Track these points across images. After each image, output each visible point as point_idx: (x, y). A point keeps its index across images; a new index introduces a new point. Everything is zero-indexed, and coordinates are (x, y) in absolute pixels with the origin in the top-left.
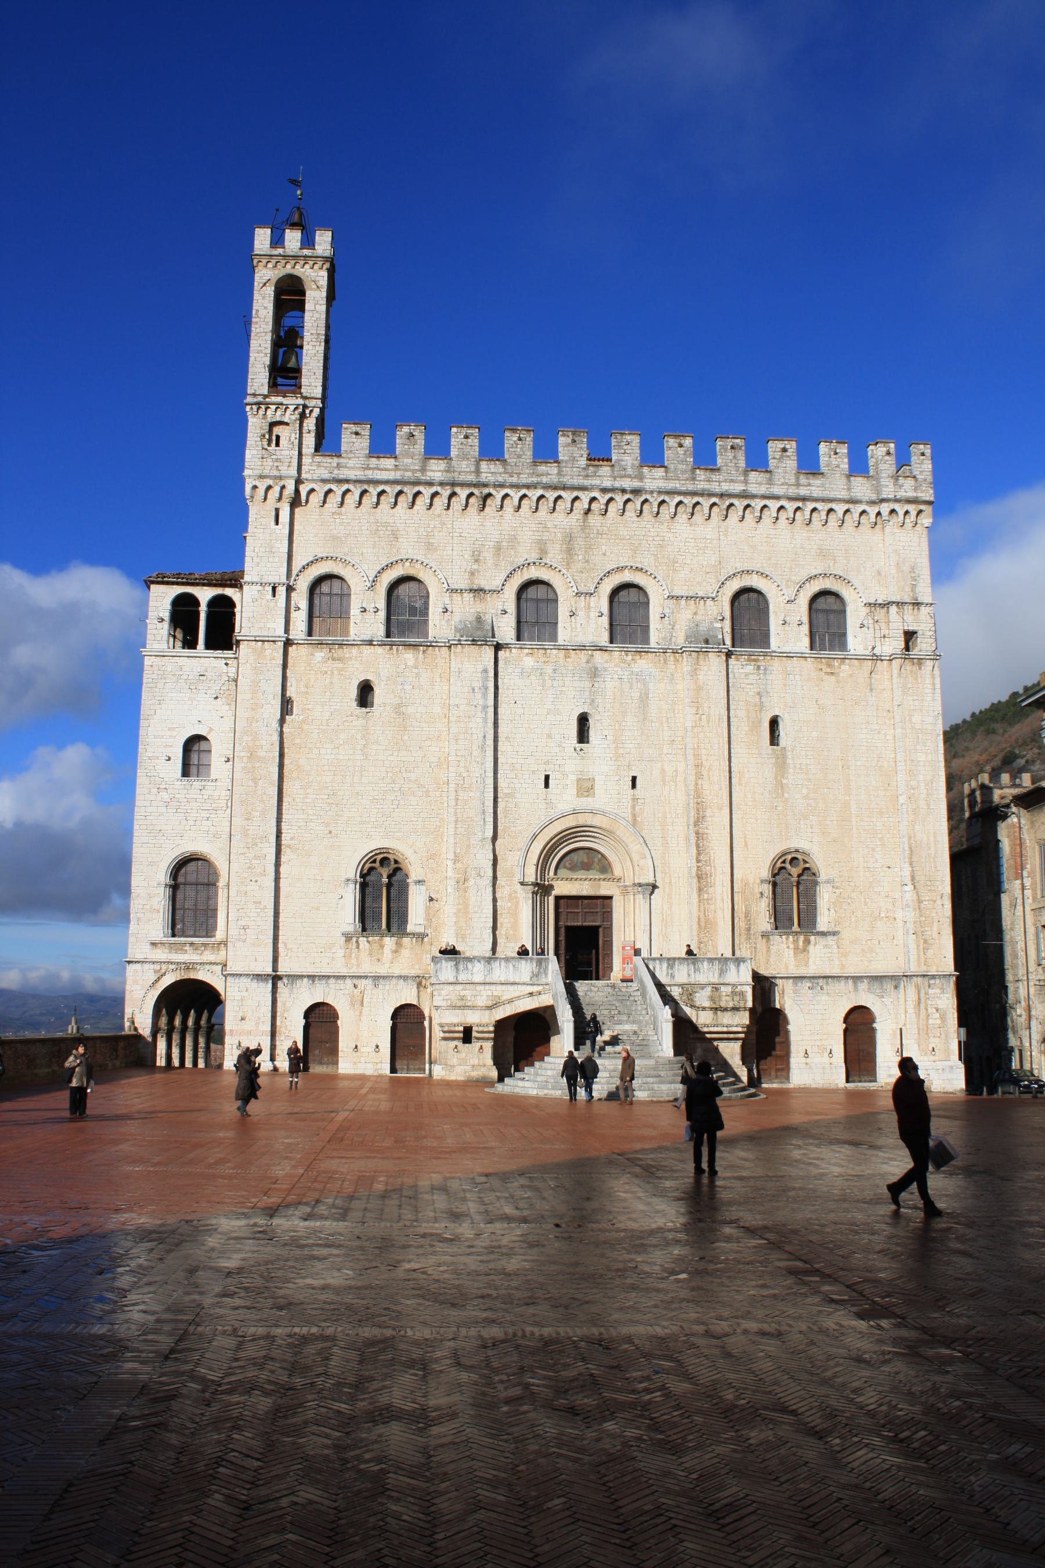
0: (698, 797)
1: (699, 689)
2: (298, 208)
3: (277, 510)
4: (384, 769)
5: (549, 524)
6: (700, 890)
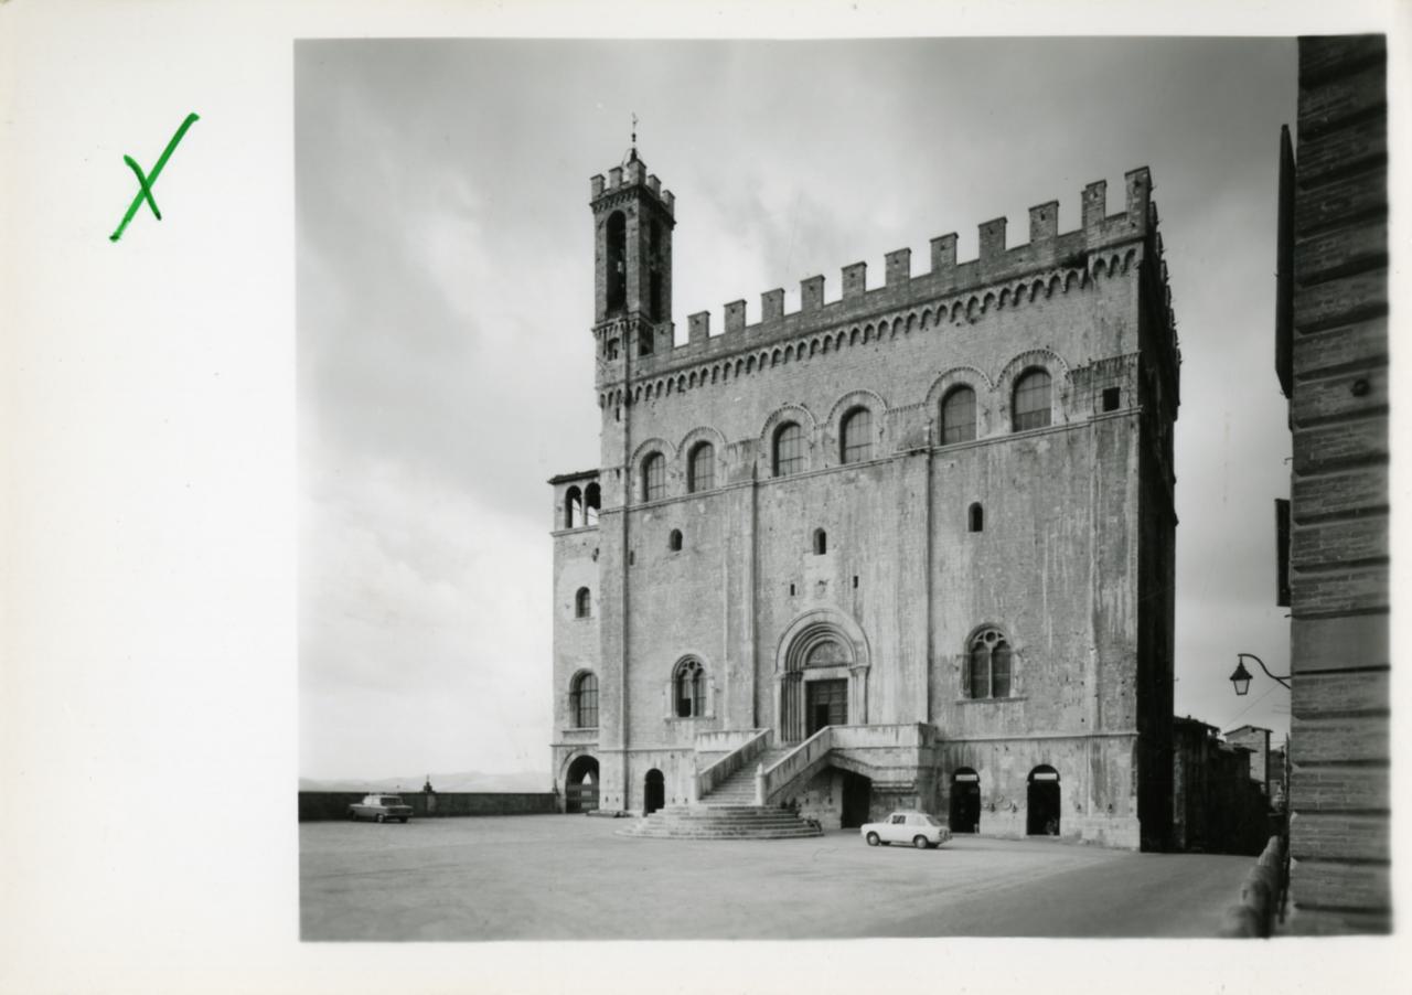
2: (634, 151)
3: (618, 410)
6: (902, 669)
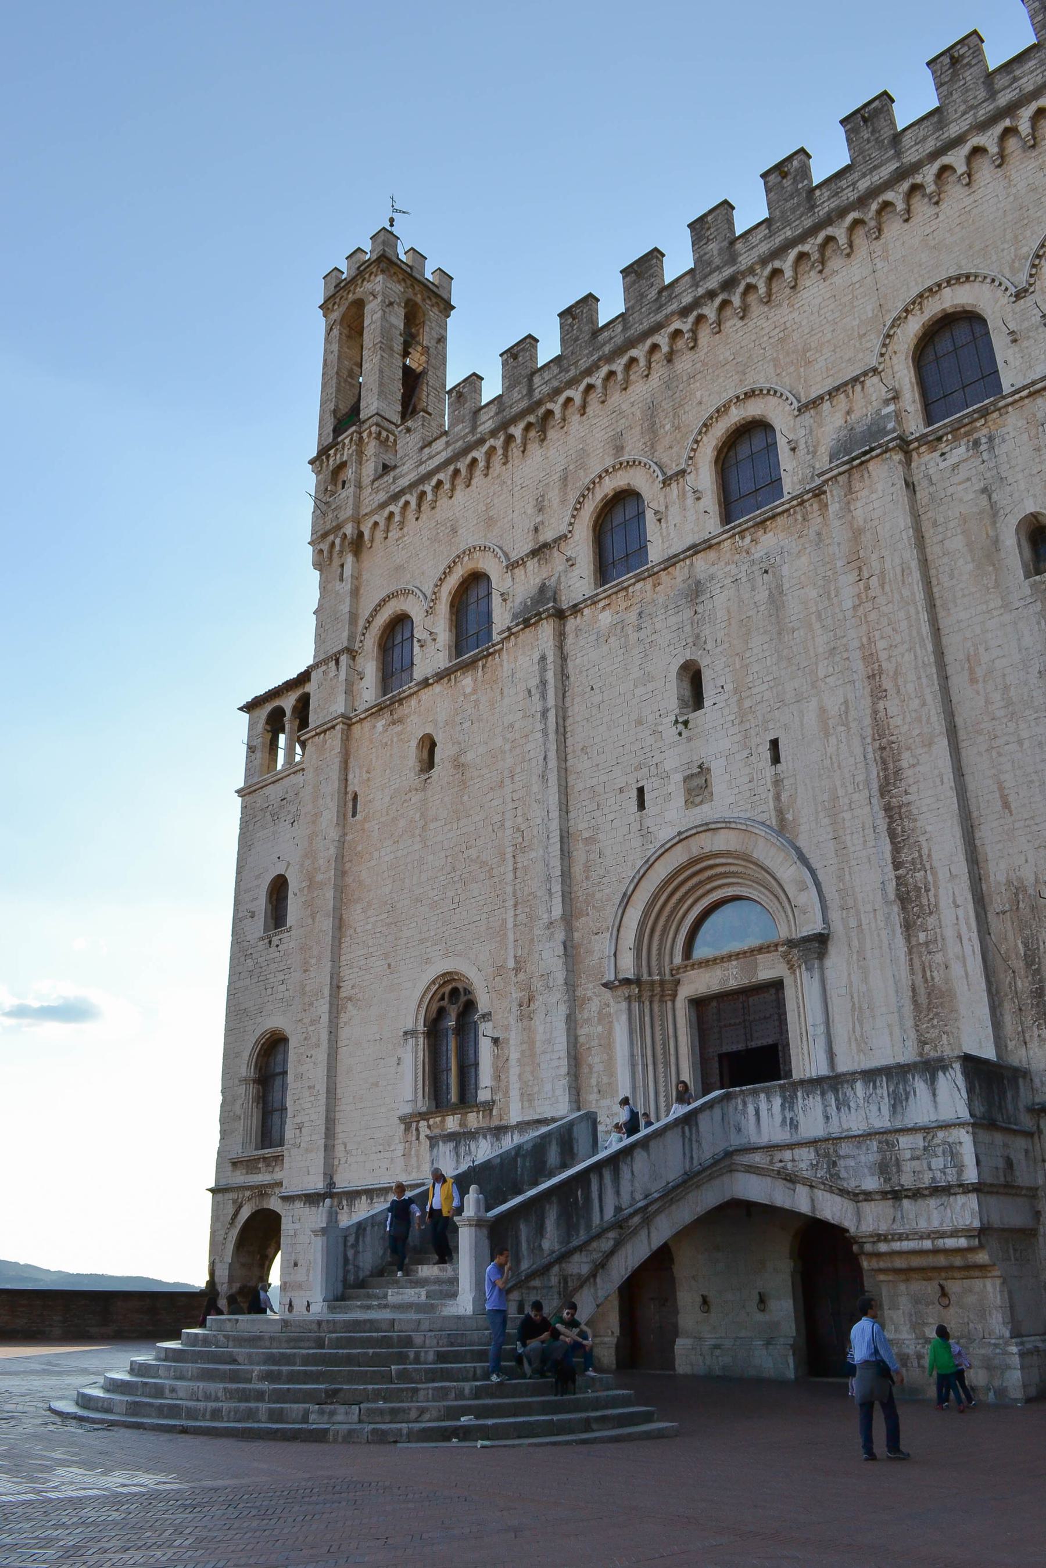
0: (881, 736)
1: (857, 534)
3: (342, 566)
4: (443, 854)
5: (624, 407)
6: (908, 927)
